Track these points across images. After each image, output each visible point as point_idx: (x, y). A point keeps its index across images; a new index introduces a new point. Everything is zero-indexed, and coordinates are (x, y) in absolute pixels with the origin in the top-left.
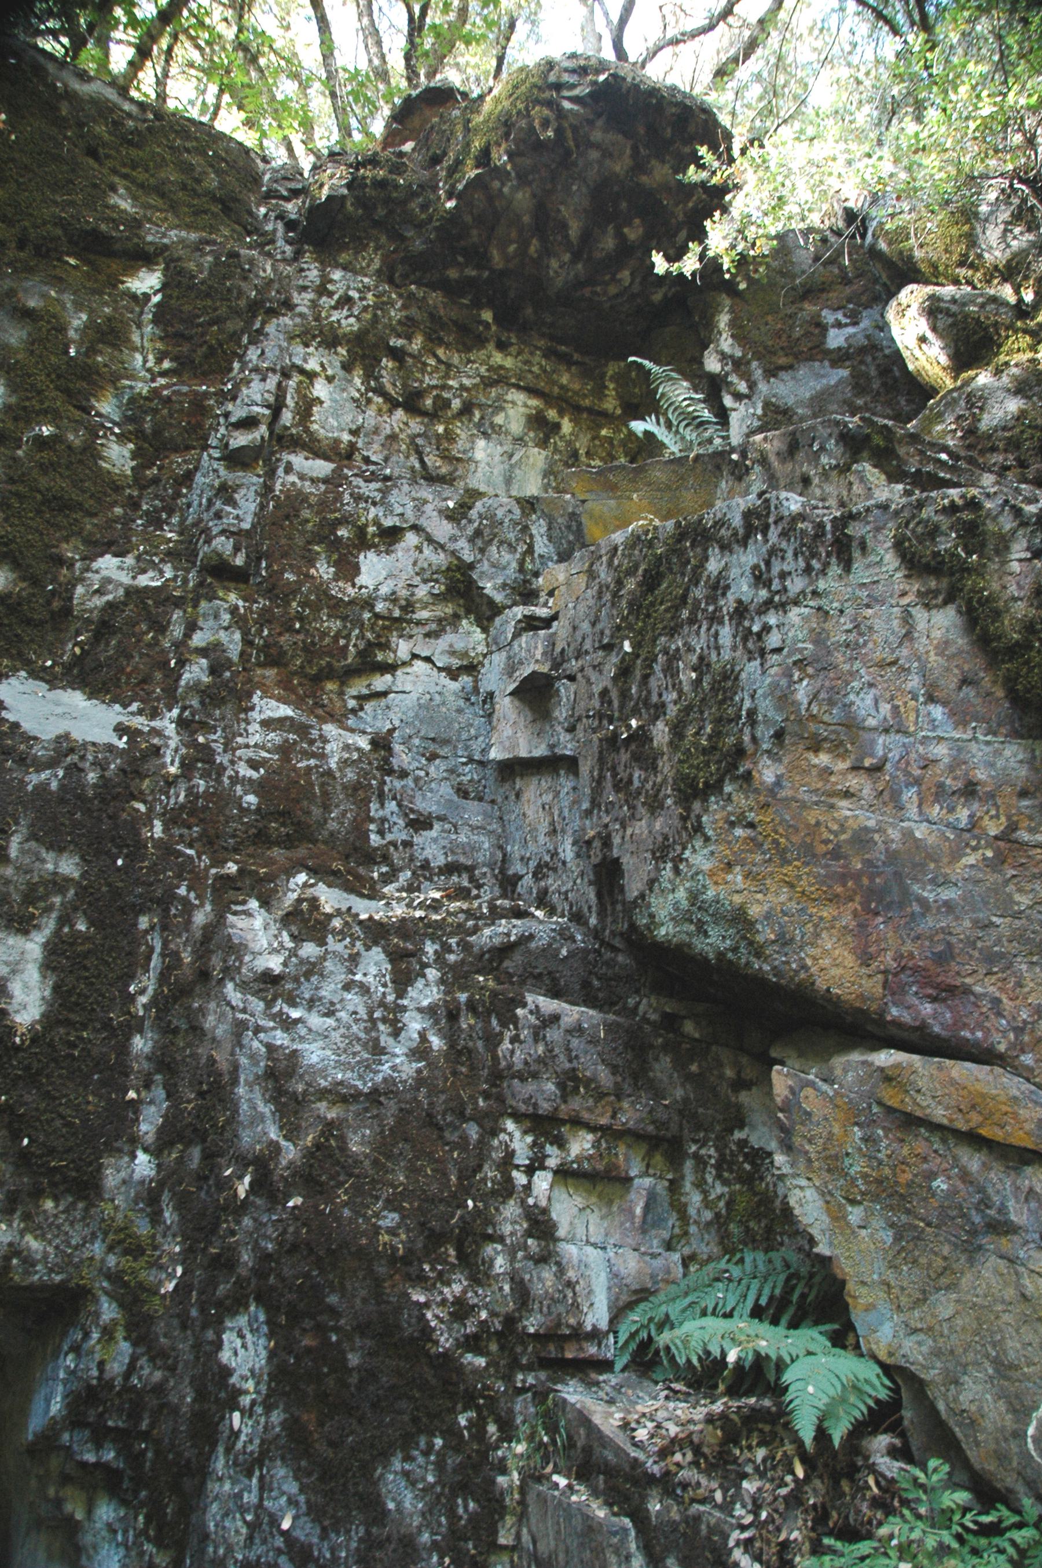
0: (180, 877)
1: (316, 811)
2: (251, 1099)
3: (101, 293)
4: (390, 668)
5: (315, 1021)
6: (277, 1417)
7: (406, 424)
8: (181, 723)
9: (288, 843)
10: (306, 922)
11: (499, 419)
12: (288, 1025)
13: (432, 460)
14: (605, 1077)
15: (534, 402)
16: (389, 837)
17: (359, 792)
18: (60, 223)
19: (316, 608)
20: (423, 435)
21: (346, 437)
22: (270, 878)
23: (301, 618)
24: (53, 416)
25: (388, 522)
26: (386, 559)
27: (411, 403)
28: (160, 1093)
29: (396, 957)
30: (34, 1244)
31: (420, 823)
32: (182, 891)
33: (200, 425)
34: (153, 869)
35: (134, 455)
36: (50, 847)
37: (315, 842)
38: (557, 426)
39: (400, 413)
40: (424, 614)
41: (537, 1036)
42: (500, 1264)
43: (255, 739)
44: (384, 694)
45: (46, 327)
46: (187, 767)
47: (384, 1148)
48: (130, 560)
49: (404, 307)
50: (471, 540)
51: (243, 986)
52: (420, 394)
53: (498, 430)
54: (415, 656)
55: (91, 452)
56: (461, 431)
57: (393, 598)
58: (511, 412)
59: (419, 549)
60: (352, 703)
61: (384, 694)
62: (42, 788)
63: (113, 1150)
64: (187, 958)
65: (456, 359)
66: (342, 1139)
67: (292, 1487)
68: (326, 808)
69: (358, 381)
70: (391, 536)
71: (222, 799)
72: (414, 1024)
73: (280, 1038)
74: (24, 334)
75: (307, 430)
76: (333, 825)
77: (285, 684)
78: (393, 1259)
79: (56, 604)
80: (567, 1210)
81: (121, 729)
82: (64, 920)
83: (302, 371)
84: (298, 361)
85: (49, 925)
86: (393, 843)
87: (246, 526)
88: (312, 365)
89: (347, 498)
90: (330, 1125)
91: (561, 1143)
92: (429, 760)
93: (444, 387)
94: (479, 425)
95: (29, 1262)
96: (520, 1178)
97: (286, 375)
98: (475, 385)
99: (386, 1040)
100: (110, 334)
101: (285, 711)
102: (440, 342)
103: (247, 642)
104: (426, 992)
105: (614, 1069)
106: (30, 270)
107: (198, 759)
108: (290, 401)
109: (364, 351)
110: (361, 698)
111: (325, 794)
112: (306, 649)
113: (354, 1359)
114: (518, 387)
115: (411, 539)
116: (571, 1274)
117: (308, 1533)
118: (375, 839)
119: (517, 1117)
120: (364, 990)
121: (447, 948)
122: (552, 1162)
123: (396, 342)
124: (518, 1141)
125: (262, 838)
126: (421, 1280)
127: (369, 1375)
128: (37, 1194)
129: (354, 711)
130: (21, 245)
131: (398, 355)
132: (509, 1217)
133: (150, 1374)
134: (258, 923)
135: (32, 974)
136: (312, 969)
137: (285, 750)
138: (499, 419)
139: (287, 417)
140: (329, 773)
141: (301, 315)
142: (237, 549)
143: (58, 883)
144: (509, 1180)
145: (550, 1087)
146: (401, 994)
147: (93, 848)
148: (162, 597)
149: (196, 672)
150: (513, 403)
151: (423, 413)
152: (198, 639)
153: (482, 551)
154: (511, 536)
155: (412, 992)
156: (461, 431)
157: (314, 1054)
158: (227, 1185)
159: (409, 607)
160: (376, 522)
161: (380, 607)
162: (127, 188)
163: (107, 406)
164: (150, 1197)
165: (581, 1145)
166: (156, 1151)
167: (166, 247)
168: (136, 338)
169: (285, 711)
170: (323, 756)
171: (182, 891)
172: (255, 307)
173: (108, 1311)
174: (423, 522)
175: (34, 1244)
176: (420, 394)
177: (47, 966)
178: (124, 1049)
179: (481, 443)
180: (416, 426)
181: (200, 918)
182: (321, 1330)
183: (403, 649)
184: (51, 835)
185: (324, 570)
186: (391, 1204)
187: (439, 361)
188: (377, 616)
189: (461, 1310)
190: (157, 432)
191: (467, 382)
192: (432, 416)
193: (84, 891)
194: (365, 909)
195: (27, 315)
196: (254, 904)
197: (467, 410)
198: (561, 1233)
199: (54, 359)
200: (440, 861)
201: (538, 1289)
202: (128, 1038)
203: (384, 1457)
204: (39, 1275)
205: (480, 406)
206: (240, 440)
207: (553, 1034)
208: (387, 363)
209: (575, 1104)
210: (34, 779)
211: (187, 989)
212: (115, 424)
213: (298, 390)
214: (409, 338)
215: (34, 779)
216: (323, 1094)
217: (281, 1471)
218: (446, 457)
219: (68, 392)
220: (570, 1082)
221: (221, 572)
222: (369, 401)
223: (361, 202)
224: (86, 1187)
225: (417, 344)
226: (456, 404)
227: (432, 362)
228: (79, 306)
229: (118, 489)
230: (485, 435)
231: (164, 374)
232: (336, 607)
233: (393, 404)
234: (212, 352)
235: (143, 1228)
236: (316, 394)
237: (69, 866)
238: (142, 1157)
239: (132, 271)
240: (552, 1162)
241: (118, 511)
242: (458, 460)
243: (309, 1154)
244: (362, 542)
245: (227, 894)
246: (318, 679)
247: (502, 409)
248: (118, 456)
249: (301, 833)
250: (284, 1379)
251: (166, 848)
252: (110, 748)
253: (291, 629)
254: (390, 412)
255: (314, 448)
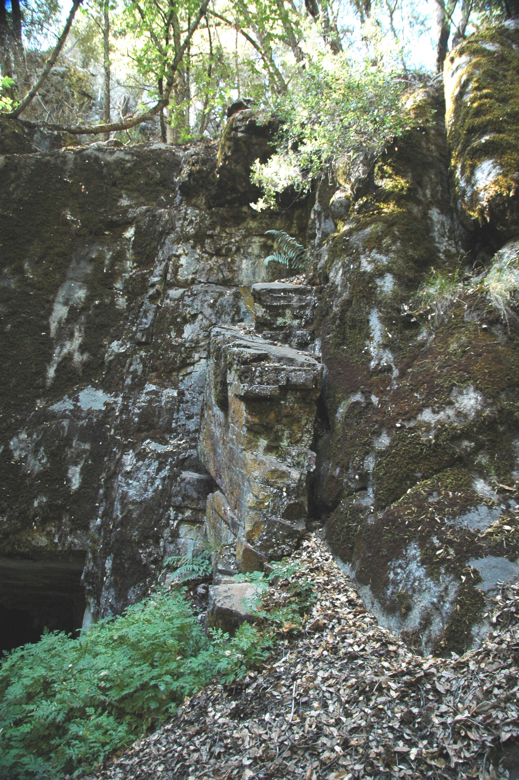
0: (115, 445)
1: (156, 420)
2: (118, 505)
3: (116, 242)
4: (193, 364)
5: (135, 483)
6: (112, 578)
7: (217, 262)
8: (123, 397)
9: (148, 430)
10: (141, 456)
11: (250, 250)
12: (128, 484)
13: (226, 273)
14: (195, 495)
15: (262, 240)
16: (179, 423)
17: (170, 411)
18: (101, 221)
19: (166, 350)
20: (224, 264)
21: (190, 277)
22: (136, 443)
23: (162, 354)
24: (100, 297)
25: (192, 313)
26: (192, 326)
27: (218, 253)
28: (104, 504)
29: (160, 463)
30: (76, 541)
31: (189, 417)
32: (114, 450)
33: (144, 286)
34: (109, 444)
35: (127, 300)
36: (83, 442)
37: (155, 429)
38: (272, 246)
39: (214, 258)
40: (203, 343)
41: (179, 485)
42: (162, 544)
43: (142, 399)
44: (191, 373)
45: (99, 262)
46: (121, 412)
47: (140, 516)
48: (120, 342)
49: (210, 218)
50: (216, 315)
51: (122, 476)
52: (220, 249)
53: (250, 254)
54: (201, 358)
55: (113, 303)
56: (237, 258)
57: (192, 341)
58: (254, 246)
59: (202, 320)
60: (181, 378)
61: (191, 373)
62: (82, 425)
63: (93, 519)
64: (112, 468)
65: (233, 231)
66: (132, 514)
67: (113, 593)
68: (159, 418)
69: (198, 251)
70: (195, 316)
71: (129, 420)
72: (158, 482)
73: (125, 489)
74: (91, 268)
75: (176, 279)
76: (161, 423)
77: (159, 377)
78: (135, 542)
79: (100, 361)
80: (184, 529)
81: (106, 404)
82: (86, 461)
83: (175, 256)
84: (174, 252)
85: (82, 462)
86: (179, 426)
87: (147, 326)
88: (180, 251)
89: (181, 306)
90: (130, 510)
91: (183, 513)
92: (200, 394)
93: (228, 244)
94: (244, 253)
95: (75, 545)
96: (171, 522)
97: (169, 259)
98: (241, 240)
99: (149, 487)
100: (119, 257)
101: (154, 387)
102: (227, 226)
103: (144, 366)
104: (164, 473)
105: (199, 493)
106: (93, 242)
107: (125, 409)
108: (170, 270)
109: (199, 239)
110: (184, 376)
111: (159, 413)
112: (164, 364)
113: (126, 566)
114: (256, 235)
115: (200, 317)
116: (180, 546)
117: (114, 603)
118: (174, 425)
119: (173, 507)
120: (148, 473)
121: (174, 460)
122: (179, 518)
123: (209, 232)
124: (172, 513)
125: (139, 430)
126: (141, 547)
127: (129, 569)
128: (76, 529)
129: (182, 381)
130: (91, 233)
131: (211, 236)
132: (166, 533)
133: (96, 569)
134: (129, 457)
135: (78, 476)
136: (138, 469)
137: (150, 402)
138: (250, 250)
139: (169, 276)
140: (161, 407)
141: (177, 232)
142: (143, 336)
143: (85, 451)
144: (168, 523)
145: (180, 498)
146: (157, 474)
147: (94, 441)
148: (124, 355)
149: (128, 381)
150: (255, 242)
151: (223, 256)
152: (132, 369)
153: (219, 318)
154: (229, 310)
155: (160, 474)
156: (237, 258)
157: (132, 492)
158: (109, 525)
159: (197, 342)
160: (189, 313)
161: (187, 345)
162: (126, 194)
163: (119, 285)
164: (99, 529)
165: (188, 513)
166: (101, 518)
167: (135, 218)
168: (128, 255)
169: (154, 387)
170: (160, 402)
171: (114, 450)
172: (162, 234)
173: (90, 555)
174: (203, 310)
175: (76, 541)
176: (220, 249)
177: (81, 474)
178: (97, 493)
179: (244, 261)
180: (221, 261)
181: (118, 456)
182: (121, 559)
183: (196, 356)
184: (83, 439)
185: (173, 334)
186: (137, 530)
187: (227, 233)
188: (187, 348)
189: (150, 554)
190: (133, 290)
191: (237, 239)
192: (226, 256)
193: (91, 453)
194: (161, 449)
195: (92, 260)
196: (131, 451)
197: (238, 250)
198: (182, 536)
199: (100, 276)
200: (194, 429)
201: (168, 550)
202: (99, 490)
203: (131, 586)
204: (78, 548)
205: (243, 247)
206: (151, 292)
207: (183, 484)
208: (208, 241)
209: (186, 503)
210: (81, 423)
211: (112, 476)
212: (121, 290)
213: (173, 265)
214: (214, 229)
215: (81, 423)
216: (131, 503)
217: (112, 590)
218: (231, 271)
219: (105, 285)
220: (185, 497)
221: (140, 344)
222: (202, 257)
223: (195, 180)
224: (86, 528)
225: (218, 229)
226: (234, 249)
227: (224, 235)
228: (109, 250)
229: (121, 314)
230: (246, 258)
231: (135, 268)
232: (174, 348)
233: (211, 255)
234: (148, 256)
235: (97, 536)
236: (181, 263)
237: (87, 446)
238: (99, 520)
239: (125, 229)
240: (179, 518)
241: (122, 322)
242: (235, 271)
243: (123, 518)
244: (185, 321)
245: (124, 449)
246: (170, 372)
247: (250, 246)
248: (122, 302)
249: (151, 427)
250: (115, 569)
251: (113, 437)
252: (100, 411)
253: (159, 359)
254: (211, 259)
255: (178, 284)
